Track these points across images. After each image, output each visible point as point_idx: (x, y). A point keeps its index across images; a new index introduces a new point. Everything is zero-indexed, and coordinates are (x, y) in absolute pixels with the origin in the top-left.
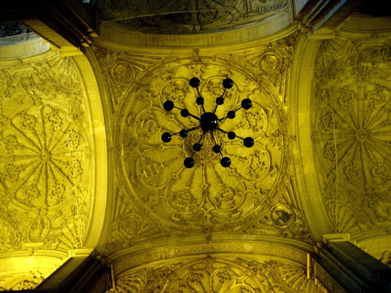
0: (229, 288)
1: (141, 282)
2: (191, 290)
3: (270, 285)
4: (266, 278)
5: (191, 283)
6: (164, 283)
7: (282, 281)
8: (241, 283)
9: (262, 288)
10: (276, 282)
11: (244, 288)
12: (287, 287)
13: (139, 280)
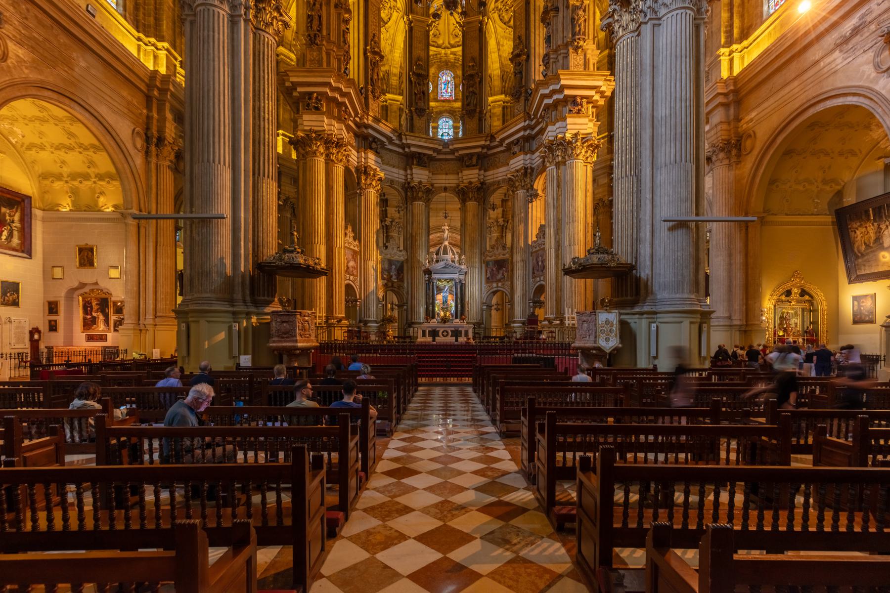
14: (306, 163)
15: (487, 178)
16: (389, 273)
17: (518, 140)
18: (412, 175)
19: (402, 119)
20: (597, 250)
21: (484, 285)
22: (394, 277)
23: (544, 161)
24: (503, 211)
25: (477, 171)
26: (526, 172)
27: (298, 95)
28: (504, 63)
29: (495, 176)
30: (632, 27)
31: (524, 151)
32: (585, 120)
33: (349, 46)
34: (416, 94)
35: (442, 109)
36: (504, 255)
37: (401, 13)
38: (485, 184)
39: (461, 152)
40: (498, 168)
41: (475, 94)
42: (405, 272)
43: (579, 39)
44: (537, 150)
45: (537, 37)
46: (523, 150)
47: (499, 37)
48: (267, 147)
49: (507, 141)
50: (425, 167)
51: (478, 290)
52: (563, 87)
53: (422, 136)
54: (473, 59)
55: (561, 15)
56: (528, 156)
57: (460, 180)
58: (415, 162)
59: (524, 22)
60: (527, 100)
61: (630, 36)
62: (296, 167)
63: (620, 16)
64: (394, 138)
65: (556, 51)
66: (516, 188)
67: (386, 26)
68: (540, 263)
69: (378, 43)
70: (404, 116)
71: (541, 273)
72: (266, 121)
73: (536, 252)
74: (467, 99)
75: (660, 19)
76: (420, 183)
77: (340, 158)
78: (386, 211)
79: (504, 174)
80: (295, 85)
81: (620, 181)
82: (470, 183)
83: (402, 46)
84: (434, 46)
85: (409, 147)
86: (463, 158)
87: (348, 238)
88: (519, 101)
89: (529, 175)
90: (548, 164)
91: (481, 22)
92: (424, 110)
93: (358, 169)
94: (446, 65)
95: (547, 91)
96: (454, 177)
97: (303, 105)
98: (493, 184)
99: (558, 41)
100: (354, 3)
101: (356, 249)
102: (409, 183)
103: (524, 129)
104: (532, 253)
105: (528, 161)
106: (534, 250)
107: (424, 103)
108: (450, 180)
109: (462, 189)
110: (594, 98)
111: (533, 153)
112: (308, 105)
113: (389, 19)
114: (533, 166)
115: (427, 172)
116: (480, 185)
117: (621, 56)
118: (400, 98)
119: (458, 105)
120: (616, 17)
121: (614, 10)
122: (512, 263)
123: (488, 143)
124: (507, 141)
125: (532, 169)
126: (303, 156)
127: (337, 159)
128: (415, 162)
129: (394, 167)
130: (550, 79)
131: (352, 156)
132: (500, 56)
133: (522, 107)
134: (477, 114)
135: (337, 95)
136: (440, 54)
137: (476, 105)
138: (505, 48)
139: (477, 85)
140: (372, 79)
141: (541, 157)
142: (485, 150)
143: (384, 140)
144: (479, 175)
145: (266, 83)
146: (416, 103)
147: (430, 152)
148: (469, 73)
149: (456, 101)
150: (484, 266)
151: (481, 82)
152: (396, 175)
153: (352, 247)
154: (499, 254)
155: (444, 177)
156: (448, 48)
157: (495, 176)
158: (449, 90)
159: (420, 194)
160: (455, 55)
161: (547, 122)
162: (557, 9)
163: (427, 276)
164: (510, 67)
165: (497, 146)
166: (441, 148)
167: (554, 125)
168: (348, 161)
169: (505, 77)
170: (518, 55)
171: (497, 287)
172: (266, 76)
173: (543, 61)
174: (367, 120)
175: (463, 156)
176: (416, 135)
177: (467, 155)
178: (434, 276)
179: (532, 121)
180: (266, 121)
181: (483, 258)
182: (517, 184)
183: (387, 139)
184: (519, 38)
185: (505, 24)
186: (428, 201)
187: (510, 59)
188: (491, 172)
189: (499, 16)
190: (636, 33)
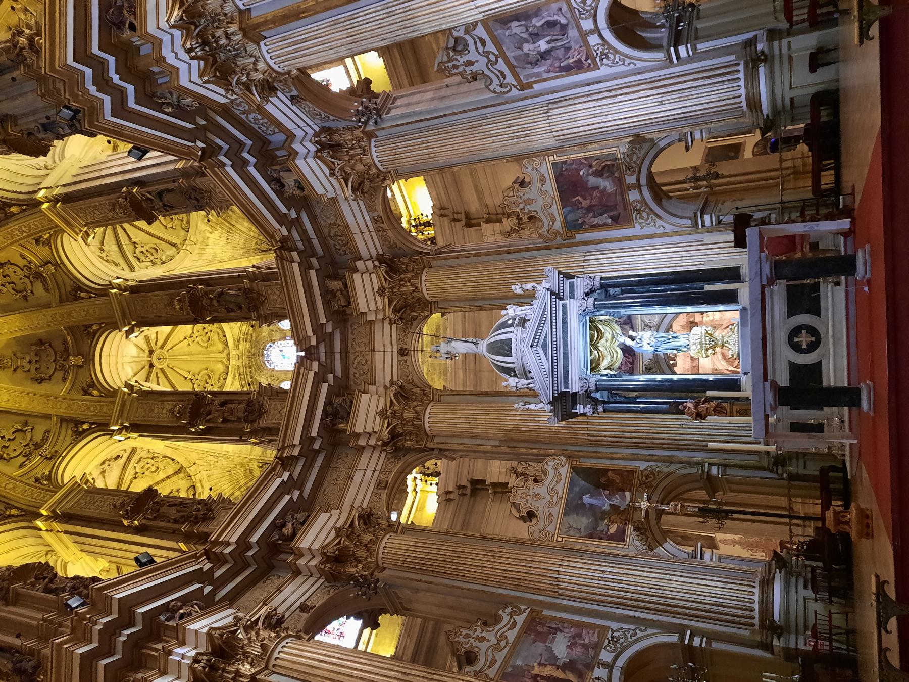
16: (604, 515)
17: (270, 180)
21: (637, 230)
22: (616, 500)
24: (488, 221)
25: (357, 277)
26: (331, 146)
28: (243, 250)
34: (225, 421)
36: (543, 180)
39: (323, 320)
41: (222, 293)
42: (603, 464)
50: (352, 402)
51: (653, 247)
52: (83, 54)
53: (285, 410)
68: (543, 45)
71: (573, 33)
73: (516, 76)
74: (232, 311)
76: (382, 414)
78: (494, 485)
82: (381, 291)
85: (313, 440)
86: (337, 312)
89: (336, 137)
90: (261, 65)
92: (250, 402)
93: (332, 578)
94: (256, 355)
96: (377, 327)
101: (520, 620)
103: (240, 166)
104: (523, 87)
106: (510, 79)
107: (240, 402)
109: (396, 311)
111: (291, 136)
113: (173, 460)
115: (365, 397)
116: (384, 266)
122: (559, 149)
128: (342, 426)
129: (350, 478)
136: (239, 367)
137: (239, 290)
138: (218, 251)
139: (209, 289)
140: (176, 521)
142: (314, 261)
150: (580, 237)
153: (512, 635)
154: (544, 193)
156: (229, 354)
159: (408, 415)
163: (580, 409)
165: (304, 234)
171: (638, 186)
174: (228, 544)
176: (283, 422)
177: (326, 303)
178: (575, 386)
179: (221, 148)
181: (559, 240)
182: (360, 167)
186: (428, 395)
189: (162, 263)
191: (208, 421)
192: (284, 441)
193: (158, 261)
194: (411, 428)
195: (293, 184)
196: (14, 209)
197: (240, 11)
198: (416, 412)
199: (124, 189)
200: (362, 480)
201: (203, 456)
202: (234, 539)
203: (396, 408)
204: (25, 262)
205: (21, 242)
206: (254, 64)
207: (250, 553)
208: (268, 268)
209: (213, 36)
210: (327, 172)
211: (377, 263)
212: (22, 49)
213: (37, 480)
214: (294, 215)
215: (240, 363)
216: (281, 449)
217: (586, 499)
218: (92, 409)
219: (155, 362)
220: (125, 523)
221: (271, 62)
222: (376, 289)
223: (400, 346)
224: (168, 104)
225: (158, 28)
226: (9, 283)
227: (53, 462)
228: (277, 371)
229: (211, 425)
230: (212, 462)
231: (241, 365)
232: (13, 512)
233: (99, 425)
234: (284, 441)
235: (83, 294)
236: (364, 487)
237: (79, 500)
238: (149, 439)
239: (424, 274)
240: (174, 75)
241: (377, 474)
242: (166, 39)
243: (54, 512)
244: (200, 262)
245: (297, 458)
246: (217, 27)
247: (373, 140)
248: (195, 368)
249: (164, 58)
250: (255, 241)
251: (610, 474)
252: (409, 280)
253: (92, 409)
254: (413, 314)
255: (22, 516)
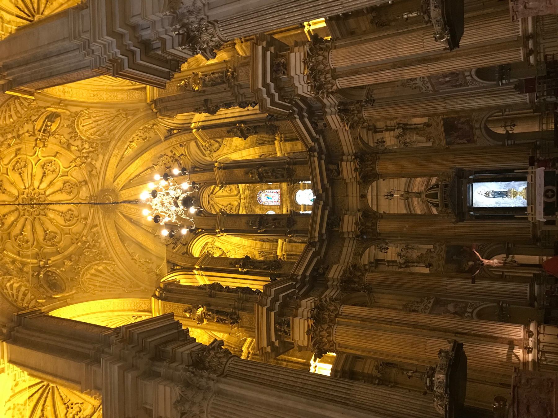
0: (12, 184)
1: (12, 282)
2: (14, 225)
3: (14, 137)
4: (5, 141)
5: (6, 227)
6: (7, 255)
7: (13, 123)
8: (7, 169)
9: (17, 147)
10: (13, 130)
11: (14, 167)
12: (21, 119)
13: (8, 284)
14: (339, 344)
15: (350, 151)
17: (312, 123)
18: (349, 232)
19: (297, 241)
20: (425, 13)
23: (332, 93)
25: (344, 164)
27: (278, 341)
28: (250, 144)
29: (348, 143)
30: (211, 31)
31: (322, 115)
32: (292, 55)
33: (238, 287)
35: (289, 201)
37: (216, 238)
38: (356, 153)
39: (326, 182)
40: (340, 141)
43: (226, 76)
44: (321, 102)
45: (227, 116)
46: (322, 117)
47: (230, 150)
48: (320, 385)
49: (314, 134)
50: (340, 219)
52: (265, 84)
54: (247, 173)
55: (210, 97)
56: (328, 110)
57: (353, 180)
58: (336, 229)
59: (217, 129)
60: (277, 119)
61: (217, 29)
62: (344, 355)
63: (204, 42)
64: (314, 249)
65: (236, 97)
66: (360, 119)
67: (225, 252)
69: (237, 261)
70: (294, 239)
72: (296, 380)
74: (278, 177)
75: (204, 5)
77: (333, 308)
79: (346, 133)
80: (270, 343)
81: (346, 5)
82: (356, 170)
83: (238, 238)
84: (239, 209)
87: (420, 309)
88: (279, 127)
89: (347, 107)
90: (335, 87)
91: (219, 168)
93: (344, 289)
94: (254, 199)
95: (268, 100)
97: (286, 337)
98: (356, 145)
99: (228, 96)
100: (209, 280)
101: (432, 301)
102: (357, 236)
103: (302, 119)
105: (333, 109)
107: (282, 219)
108: (354, 190)
109: (362, 178)
110: (273, 52)
111: (324, 105)
112: (286, 333)
113: (220, 249)
114: (337, 103)
115: (346, 217)
117: (233, 33)
118: (280, 241)
119: (284, 185)
120: (205, 46)
121: (200, 49)
122: (446, 114)
123: (316, 154)
124: (314, 134)
125: (341, 104)
126: (332, 346)
127: (335, 310)
128: (336, 229)
129: (341, 251)
130: (258, 98)
131: (331, 294)
132: (245, 148)
133: (283, 122)
134: (291, 167)
135: (278, 303)
138: (238, 145)
139: (266, 168)
141: (328, 96)
142: (323, 156)
143: (316, 259)
144: (348, 161)
145: (265, 373)
146: (283, 226)
147: (326, 213)
148: (257, 177)
149: (281, 188)
151: (264, 165)
152: (350, 249)
153: (430, 305)
155: (350, 198)
156: (240, 196)
157: (348, 143)
158: (273, 195)
159: (369, 224)
160: (245, 190)
161: (295, 96)
162: (206, 101)
164: (251, 138)
166: (322, 202)
167: (297, 87)
168: (336, 299)
169: (260, 142)
170: (242, 131)
172: (259, 372)
173: (244, 108)
174: (298, 276)
175: (329, 180)
177: (328, 175)
179: (294, 111)
180: (296, 380)
182: (356, 118)
183: (316, 257)
184: (228, 132)
185: (220, 146)
187: (245, 139)
188: (345, 148)
189: (215, 151)
190: (216, 24)
191: (266, 227)
192: (311, 235)
193: (212, 151)
194: (370, 230)
195: (322, 125)
196: (175, 131)
197: (331, 69)
198: (373, 223)
199: (237, 125)
200: (347, 252)
201: (233, 247)
202: (300, 273)
203: (362, 221)
204: (172, 155)
205: (175, 146)
206: (332, 87)
207: (307, 279)
208: (295, 159)
209: (319, 77)
210: (340, 120)
211: (353, 157)
212: (229, 77)
213: (182, 254)
214: (318, 137)
215: (245, 201)
216: (310, 238)
217: (455, 257)
218: (203, 222)
219: (210, 200)
220: (240, 270)
221: (339, 86)
222: (353, 169)
223: (361, 194)
224: (287, 99)
225: (296, 74)
226: (164, 164)
227: (186, 246)
228: (265, 205)
229: (268, 229)
230: (236, 251)
231: (246, 202)
232: (178, 267)
233: (206, 230)
234: (311, 235)
235: (197, 169)
236: (348, 255)
237: (210, 262)
238: (230, 236)
239: (377, 162)
240: (296, 89)
241: (353, 249)
242: (296, 77)
243: (201, 267)
244: (230, 150)
245: (316, 242)
246: (321, 75)
247: (363, 108)
248: (225, 204)
249: (294, 84)
250: (255, 139)
251: (464, 247)
252: (370, 165)
253: (203, 222)
254: (369, 179)
255: (182, 269)
